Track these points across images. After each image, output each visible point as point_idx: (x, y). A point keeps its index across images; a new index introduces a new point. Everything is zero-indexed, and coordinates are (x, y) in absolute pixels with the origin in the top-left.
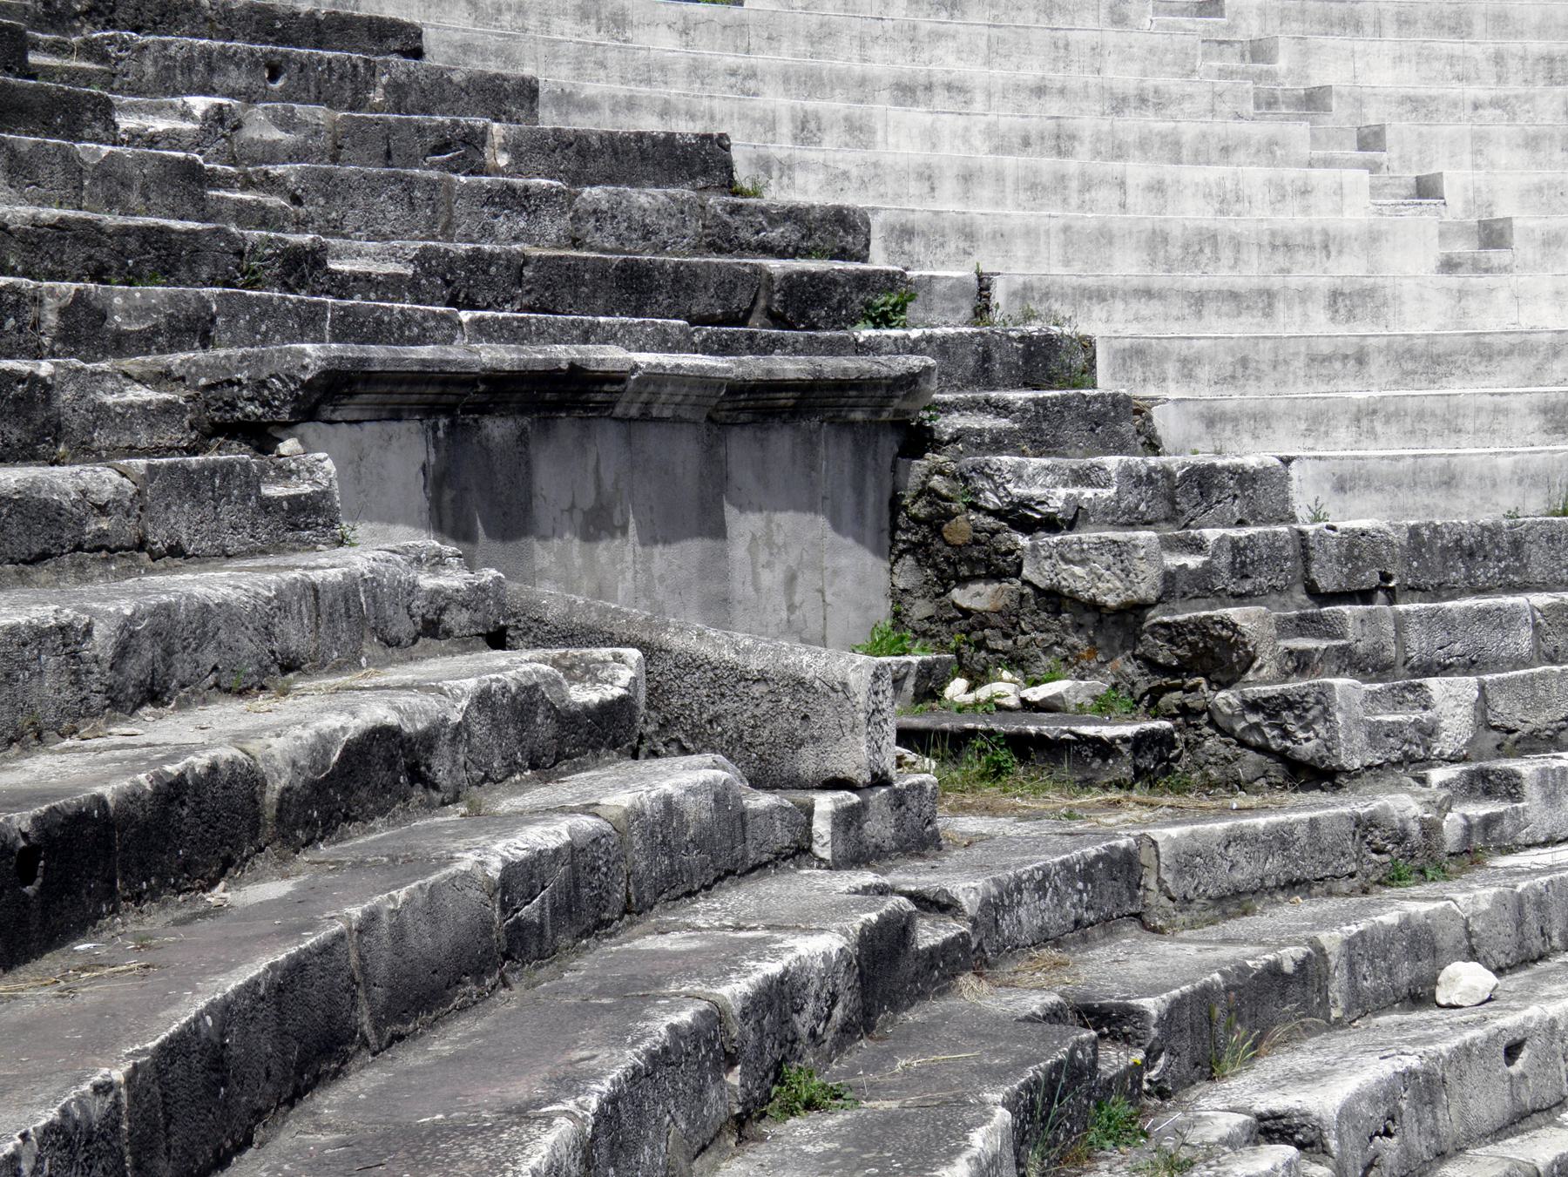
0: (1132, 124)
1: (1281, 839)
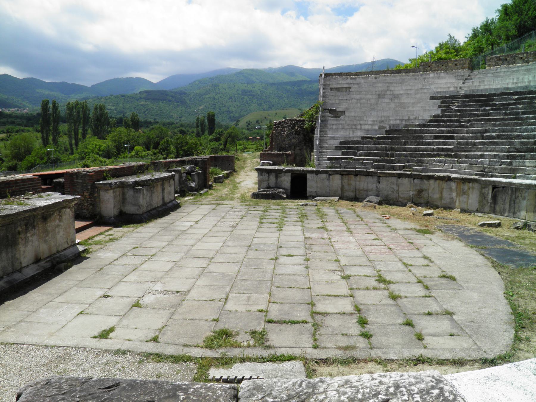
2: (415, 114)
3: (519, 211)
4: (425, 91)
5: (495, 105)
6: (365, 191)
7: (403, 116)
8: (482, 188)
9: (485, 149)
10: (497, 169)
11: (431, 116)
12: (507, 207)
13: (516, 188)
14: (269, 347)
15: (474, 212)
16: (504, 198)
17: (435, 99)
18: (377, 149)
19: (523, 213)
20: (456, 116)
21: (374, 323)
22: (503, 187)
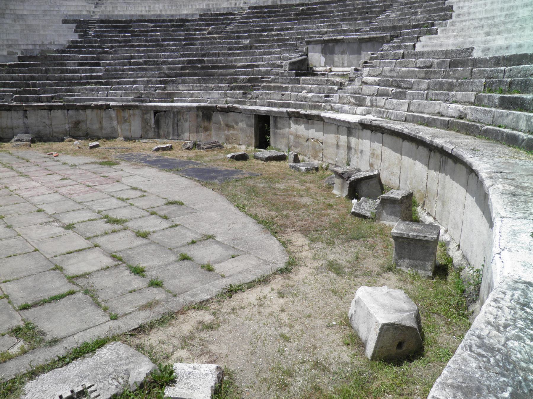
1: (317, 80)
2: (48, 38)
3: (183, 133)
4: (55, 13)
5: (134, 31)
6: (10, 128)
7: (34, 41)
8: (143, 114)
9: (135, 75)
10: (153, 94)
11: (68, 41)
12: (171, 130)
13: (177, 111)
14: (55, 342)
15: (138, 138)
16: (167, 122)
17: (68, 23)
18: (12, 79)
19: (187, 135)
20: (96, 42)
21: (151, 268)
22: (165, 111)
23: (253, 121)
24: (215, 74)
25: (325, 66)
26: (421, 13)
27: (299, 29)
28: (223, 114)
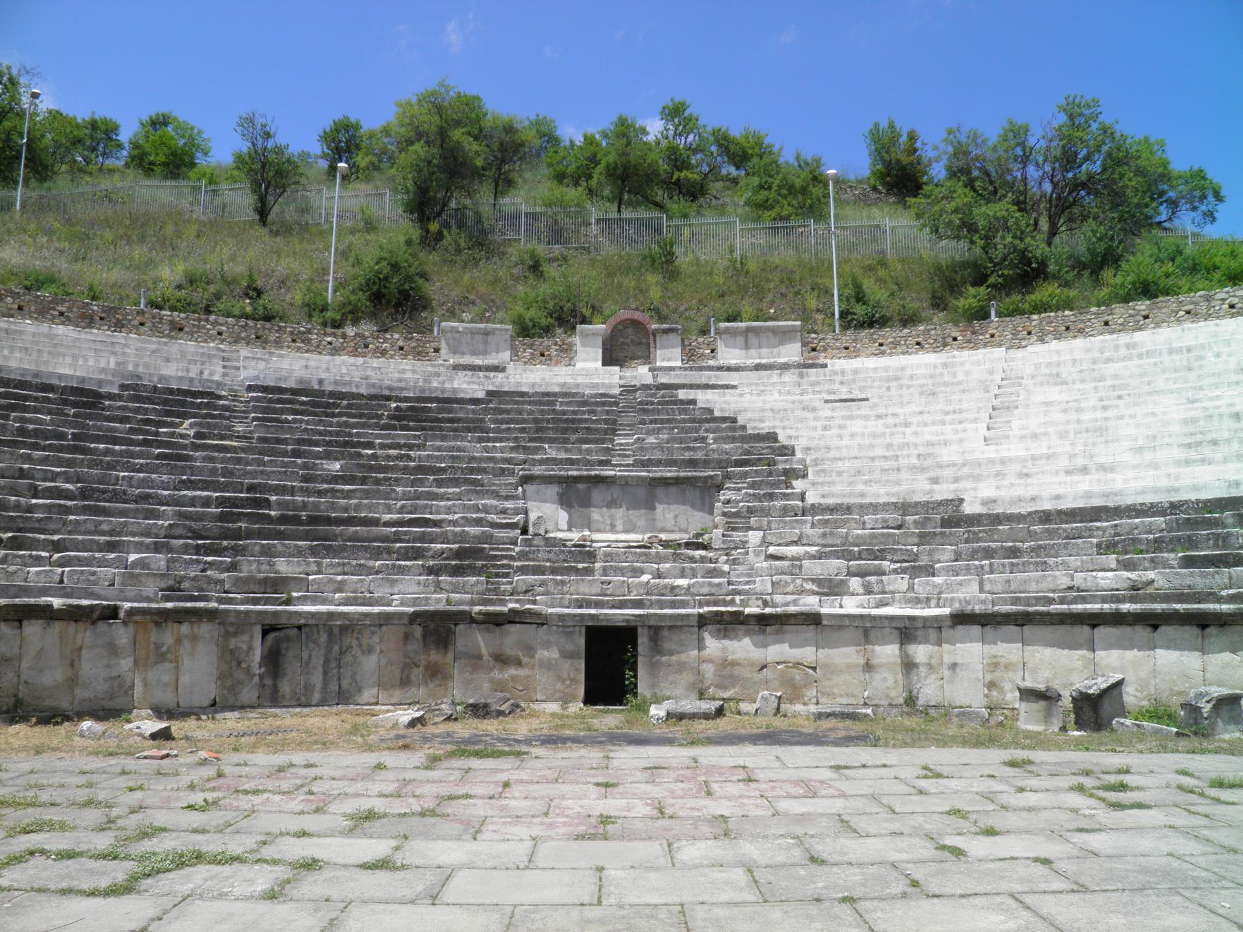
0: (948, 418)
8: (227, 635)
9: (91, 527)
12: (317, 678)
15: (203, 710)
16: (305, 655)
22: (299, 628)
23: (582, 641)
24: (336, 536)
25: (569, 530)
26: (715, 440)
27: (439, 449)
28: (488, 630)
